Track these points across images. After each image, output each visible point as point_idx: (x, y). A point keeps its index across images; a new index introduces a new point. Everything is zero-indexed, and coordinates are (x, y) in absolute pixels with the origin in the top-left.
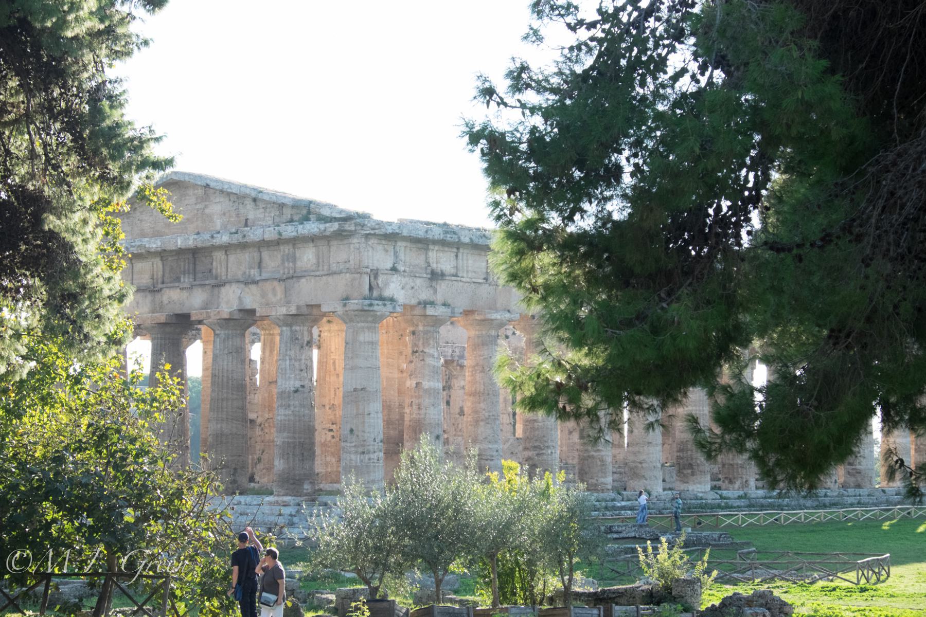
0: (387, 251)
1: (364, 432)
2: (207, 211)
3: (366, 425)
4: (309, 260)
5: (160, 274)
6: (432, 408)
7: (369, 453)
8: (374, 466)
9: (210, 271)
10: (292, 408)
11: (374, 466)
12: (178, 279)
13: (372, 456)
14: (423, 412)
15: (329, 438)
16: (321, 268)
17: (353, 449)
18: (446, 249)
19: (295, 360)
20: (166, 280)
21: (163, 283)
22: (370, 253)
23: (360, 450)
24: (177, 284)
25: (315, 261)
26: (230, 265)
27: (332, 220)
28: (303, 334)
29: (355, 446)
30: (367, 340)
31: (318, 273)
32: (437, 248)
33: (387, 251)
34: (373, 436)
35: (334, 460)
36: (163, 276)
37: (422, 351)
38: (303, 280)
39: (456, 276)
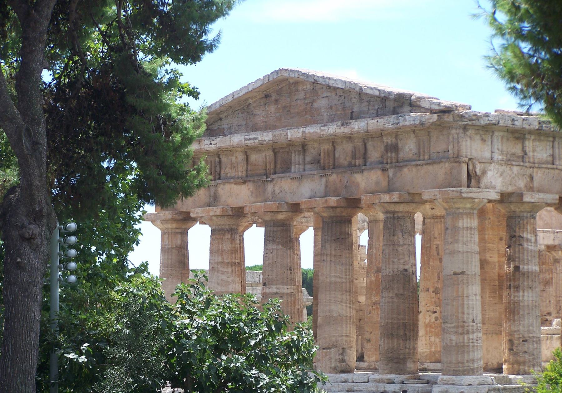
0: (485, 141)
1: (463, 313)
2: (315, 105)
3: (466, 306)
4: (411, 150)
6: (530, 291)
7: (468, 333)
8: (473, 346)
11: (473, 346)
13: (471, 337)
15: (433, 320)
16: (422, 158)
18: (542, 138)
20: (277, 170)
22: (468, 143)
23: (460, 330)
24: (288, 175)
25: (415, 150)
27: (432, 112)
30: (465, 226)
31: (419, 162)
32: (533, 137)
34: (471, 317)
35: (437, 340)
36: (275, 167)
37: (520, 236)
38: (406, 170)
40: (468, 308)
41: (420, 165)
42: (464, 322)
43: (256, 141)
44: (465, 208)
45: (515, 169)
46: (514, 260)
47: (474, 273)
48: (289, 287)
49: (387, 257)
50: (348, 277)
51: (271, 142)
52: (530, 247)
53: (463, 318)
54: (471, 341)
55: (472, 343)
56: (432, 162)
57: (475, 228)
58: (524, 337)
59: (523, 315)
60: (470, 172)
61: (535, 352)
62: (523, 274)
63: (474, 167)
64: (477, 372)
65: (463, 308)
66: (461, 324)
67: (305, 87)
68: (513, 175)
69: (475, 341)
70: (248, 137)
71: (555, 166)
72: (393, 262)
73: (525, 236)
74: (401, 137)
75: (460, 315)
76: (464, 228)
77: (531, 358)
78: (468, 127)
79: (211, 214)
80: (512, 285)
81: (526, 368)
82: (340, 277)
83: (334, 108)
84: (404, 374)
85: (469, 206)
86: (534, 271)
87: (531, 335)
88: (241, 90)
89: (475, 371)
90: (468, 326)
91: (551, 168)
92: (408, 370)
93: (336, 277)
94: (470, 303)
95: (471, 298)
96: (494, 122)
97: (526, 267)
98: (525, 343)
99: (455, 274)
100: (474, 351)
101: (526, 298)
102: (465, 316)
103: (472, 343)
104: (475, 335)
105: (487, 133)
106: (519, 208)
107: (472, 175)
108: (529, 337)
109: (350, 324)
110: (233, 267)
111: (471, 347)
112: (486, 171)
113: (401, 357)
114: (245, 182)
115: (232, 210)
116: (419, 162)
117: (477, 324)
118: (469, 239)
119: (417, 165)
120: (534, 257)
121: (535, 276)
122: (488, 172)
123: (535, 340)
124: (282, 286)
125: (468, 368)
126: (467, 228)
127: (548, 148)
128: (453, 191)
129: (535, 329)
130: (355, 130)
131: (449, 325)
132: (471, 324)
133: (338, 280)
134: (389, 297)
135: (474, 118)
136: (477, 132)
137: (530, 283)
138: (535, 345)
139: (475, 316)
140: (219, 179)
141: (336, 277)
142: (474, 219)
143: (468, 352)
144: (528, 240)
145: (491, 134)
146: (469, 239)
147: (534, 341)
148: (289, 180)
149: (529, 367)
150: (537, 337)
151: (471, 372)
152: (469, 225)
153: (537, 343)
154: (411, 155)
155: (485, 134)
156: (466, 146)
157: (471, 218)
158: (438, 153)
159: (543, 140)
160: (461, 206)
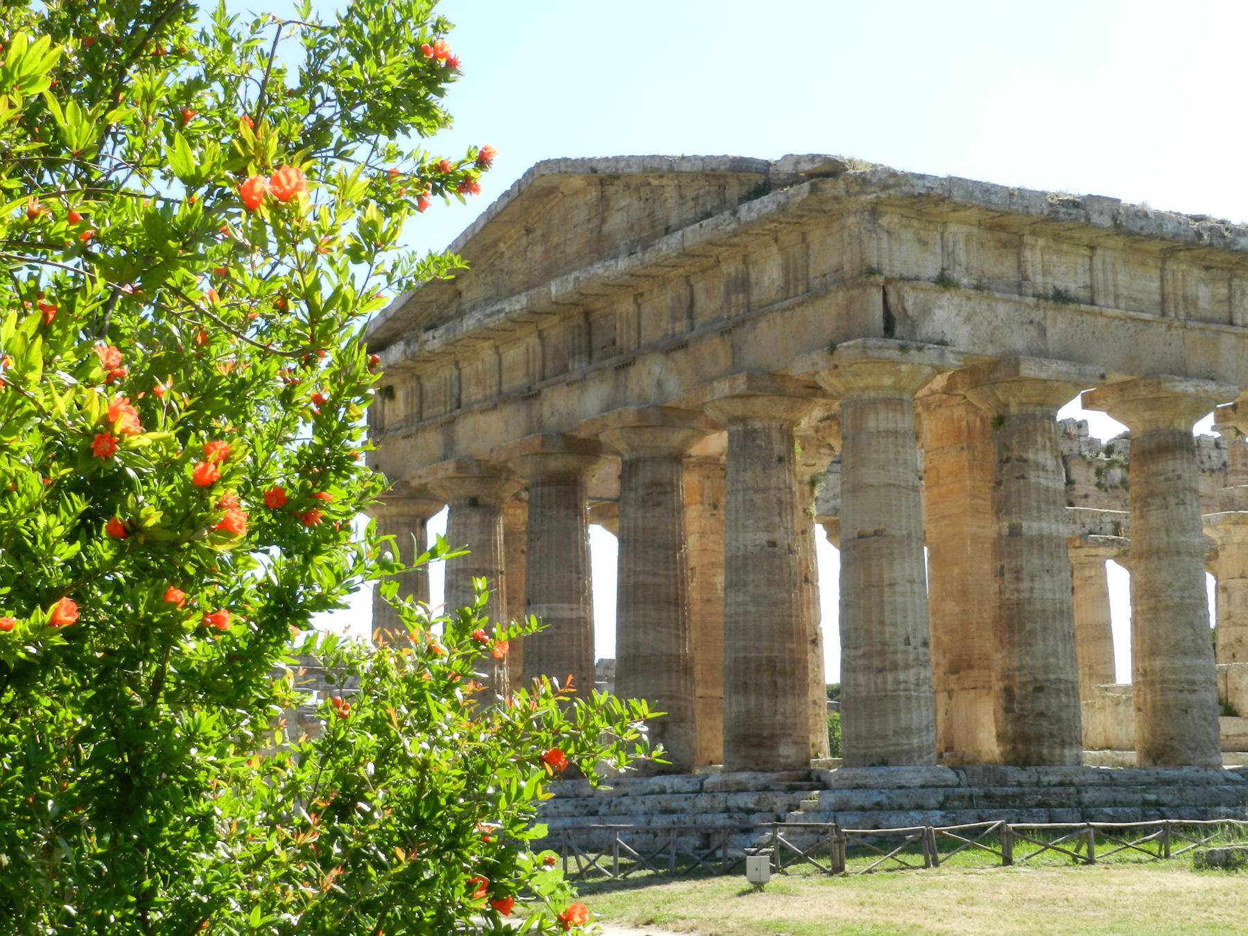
1: (882, 623)
2: (606, 229)
3: (887, 608)
5: (538, 363)
6: (1047, 578)
7: (895, 667)
8: (909, 698)
9: (614, 343)
10: (751, 589)
11: (909, 698)
12: (565, 369)
13: (902, 676)
14: (1025, 585)
16: (792, 292)
17: (861, 662)
18: (1065, 247)
19: (756, 491)
20: (548, 372)
21: (543, 379)
22: (884, 244)
23: (876, 662)
24: (562, 377)
25: (780, 282)
26: (643, 323)
28: (769, 436)
29: (865, 656)
30: (882, 426)
31: (786, 303)
32: (1041, 242)
33: (926, 244)
36: (544, 367)
37: (1021, 459)
38: (763, 325)
39: (1092, 303)
40: (894, 611)
41: (788, 309)
42: (884, 644)
43: (502, 315)
44: (881, 388)
45: (1002, 310)
46: (1009, 513)
47: (905, 532)
48: (575, 606)
49: (733, 517)
50: (672, 573)
51: (525, 311)
52: (1042, 481)
53: (882, 633)
54: (902, 686)
55: (906, 690)
56: (813, 295)
57: (905, 434)
58: (1035, 680)
59: (1032, 633)
60: (893, 310)
61: (1064, 715)
62: (1030, 541)
63: (901, 299)
64: (920, 757)
65: (882, 611)
66: (879, 647)
67: (589, 197)
68: (997, 322)
69: (912, 687)
70: (488, 311)
71: (1096, 308)
72: (744, 526)
73: (1031, 456)
74: (754, 257)
75: (875, 628)
76: (879, 432)
77: (1056, 727)
78: (881, 208)
79: (441, 474)
80: (1006, 566)
81: (1045, 751)
82: (655, 575)
83: (636, 228)
84: (772, 771)
85: (888, 381)
86: (1055, 534)
87: (1052, 677)
88: (478, 220)
89: (916, 754)
90: (895, 652)
91: (1087, 312)
92: (781, 760)
93: (645, 573)
94: (899, 599)
95: (899, 588)
96: (940, 191)
97: (1035, 525)
98: (1040, 694)
99: (862, 536)
100: (909, 710)
101: (1037, 594)
102: (888, 630)
103: (906, 690)
104: (912, 672)
105: (932, 227)
106: (1014, 396)
107: (896, 316)
108: (1048, 680)
109: (678, 671)
111: (903, 699)
112: (930, 309)
113: (766, 733)
114: (495, 407)
115: (479, 466)
116: (786, 303)
117: (915, 648)
118: (892, 456)
119: (783, 310)
120: (1055, 502)
121: (1058, 546)
122: (937, 311)
123: (1062, 686)
124: (559, 605)
125: (899, 748)
127: (1080, 270)
128: (848, 347)
129: (1061, 663)
130: (662, 253)
132: (902, 647)
133: (650, 579)
134: (738, 604)
135: (891, 181)
136: (904, 221)
137: (1047, 560)
138: (1064, 699)
139: (910, 629)
140: (459, 407)
141: (645, 573)
142: (903, 413)
143: (896, 711)
144: (1040, 467)
145: (940, 230)
146: (892, 456)
147: (1060, 690)
148: (565, 389)
149: (1051, 748)
150: (1067, 681)
151: (904, 758)
152: (891, 426)
153: (1067, 694)
154: (773, 293)
155: (925, 229)
156: (879, 249)
157: (895, 410)
158: (824, 275)
159: (1068, 252)
160: (870, 381)
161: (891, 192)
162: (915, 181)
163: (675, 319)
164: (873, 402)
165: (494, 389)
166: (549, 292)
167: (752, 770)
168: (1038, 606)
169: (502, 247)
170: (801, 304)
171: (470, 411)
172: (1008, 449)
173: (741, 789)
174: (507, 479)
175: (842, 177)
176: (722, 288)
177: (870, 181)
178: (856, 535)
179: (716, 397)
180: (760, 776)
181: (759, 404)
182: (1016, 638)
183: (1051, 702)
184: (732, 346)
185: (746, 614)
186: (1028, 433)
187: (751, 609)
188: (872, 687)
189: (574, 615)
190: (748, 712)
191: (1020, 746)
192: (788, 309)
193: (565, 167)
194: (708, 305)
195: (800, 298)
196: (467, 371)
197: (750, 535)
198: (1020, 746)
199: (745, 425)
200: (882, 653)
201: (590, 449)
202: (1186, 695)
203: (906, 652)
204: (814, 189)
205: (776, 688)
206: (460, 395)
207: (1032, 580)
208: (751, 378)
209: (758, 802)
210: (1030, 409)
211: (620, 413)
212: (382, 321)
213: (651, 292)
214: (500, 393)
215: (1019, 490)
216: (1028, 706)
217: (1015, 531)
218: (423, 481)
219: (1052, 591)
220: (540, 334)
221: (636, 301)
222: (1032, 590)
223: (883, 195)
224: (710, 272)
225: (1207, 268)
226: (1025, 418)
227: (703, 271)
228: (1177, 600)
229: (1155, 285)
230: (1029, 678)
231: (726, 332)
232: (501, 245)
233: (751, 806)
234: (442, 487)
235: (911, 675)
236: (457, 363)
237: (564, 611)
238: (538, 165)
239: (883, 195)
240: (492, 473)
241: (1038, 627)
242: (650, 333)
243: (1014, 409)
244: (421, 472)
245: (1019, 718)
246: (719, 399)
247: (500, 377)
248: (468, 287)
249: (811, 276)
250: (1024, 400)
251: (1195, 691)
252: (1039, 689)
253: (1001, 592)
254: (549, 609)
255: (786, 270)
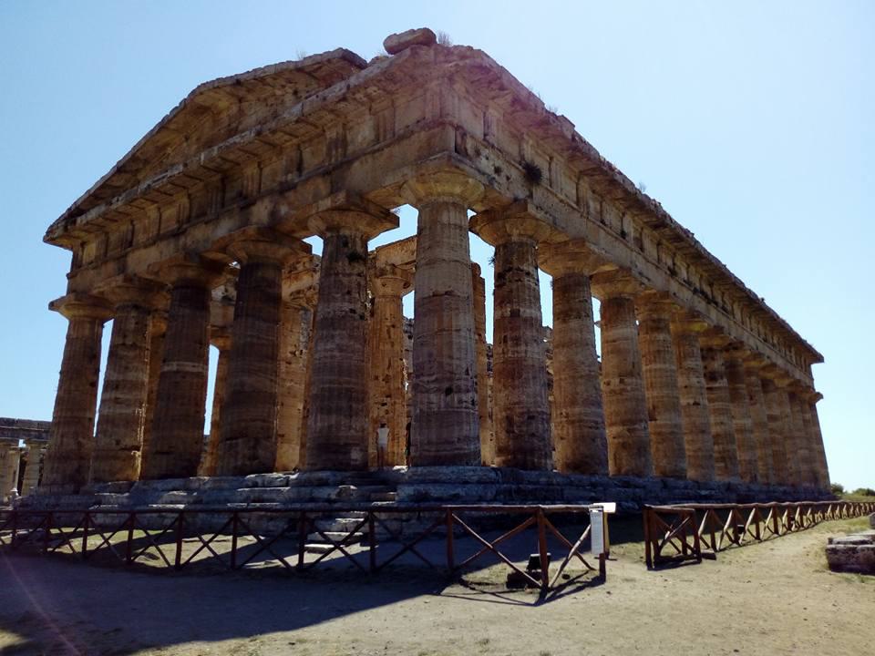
1: (451, 357)
3: (455, 347)
7: (459, 391)
10: (337, 340)
14: (523, 348)
19: (344, 275)
24: (203, 219)
25: (372, 137)
28: (354, 241)
29: (436, 380)
37: (518, 269)
38: (356, 164)
41: (378, 150)
42: (451, 373)
43: (165, 180)
44: (452, 195)
46: (510, 302)
53: (451, 365)
54: (464, 404)
55: (466, 408)
59: (527, 380)
61: (546, 436)
62: (525, 320)
65: (451, 348)
66: (448, 375)
75: (446, 360)
79: (114, 284)
80: (508, 336)
84: (346, 471)
85: (458, 190)
87: (539, 410)
92: (352, 463)
95: (463, 334)
97: (528, 311)
100: (469, 423)
101: (529, 354)
102: (455, 362)
104: (470, 394)
108: (537, 412)
110: (138, 352)
113: (342, 443)
114: (154, 243)
118: (458, 242)
119: (374, 152)
123: (545, 417)
125: (462, 452)
126: (455, 225)
131: (426, 379)
132: (465, 376)
134: (326, 350)
137: (535, 334)
147: (543, 419)
149: (540, 458)
152: (458, 222)
160: (447, 188)
161: (468, 61)
162: (485, 58)
163: (288, 172)
164: (446, 203)
165: (155, 233)
166: (200, 159)
167: (330, 470)
168: (530, 362)
169: (169, 150)
170: (388, 146)
171: (138, 248)
172: (511, 263)
173: (323, 483)
174: (158, 292)
175: (433, 47)
176: (325, 149)
177: (452, 53)
178: (431, 294)
179: (320, 210)
180: (338, 474)
181: (349, 218)
182: (517, 382)
183: (537, 426)
184: (331, 183)
185: (332, 357)
186: (523, 254)
187: (336, 353)
188: (443, 405)
189: (195, 370)
190: (330, 427)
191: (519, 456)
192: (378, 150)
193: (217, 86)
194: (311, 161)
195: (388, 142)
196: (138, 226)
197: (338, 304)
198: (519, 456)
199: (338, 232)
200: (450, 379)
201: (217, 268)
202: (593, 430)
203: (467, 380)
204: (414, 53)
205: (351, 410)
206: (132, 239)
207: (527, 346)
208: (348, 196)
209: (339, 494)
210: (524, 239)
211: (244, 231)
212: (87, 195)
213: (271, 159)
214: (158, 234)
215: (518, 288)
216: (525, 429)
217: (515, 314)
218: (101, 290)
219: (538, 353)
220: (189, 196)
221: (259, 165)
222: (526, 352)
223: (461, 63)
224: (316, 140)
225: (594, 192)
226: (521, 244)
227: (311, 140)
228: (587, 372)
229: (574, 192)
230: (525, 410)
231: (327, 173)
232: (169, 149)
233: (333, 497)
234: (114, 293)
235: (467, 397)
236: (132, 222)
237: (189, 367)
238: (199, 87)
239: (461, 63)
240: (148, 287)
241: (530, 376)
242: (267, 184)
243: (515, 238)
244: (101, 284)
245: (517, 438)
246: (323, 211)
247: (160, 226)
248: (144, 177)
249: (396, 130)
250: (522, 232)
251: (597, 428)
252: (531, 418)
253: (504, 353)
254: (178, 365)
255: (377, 128)
